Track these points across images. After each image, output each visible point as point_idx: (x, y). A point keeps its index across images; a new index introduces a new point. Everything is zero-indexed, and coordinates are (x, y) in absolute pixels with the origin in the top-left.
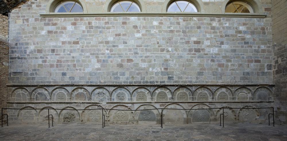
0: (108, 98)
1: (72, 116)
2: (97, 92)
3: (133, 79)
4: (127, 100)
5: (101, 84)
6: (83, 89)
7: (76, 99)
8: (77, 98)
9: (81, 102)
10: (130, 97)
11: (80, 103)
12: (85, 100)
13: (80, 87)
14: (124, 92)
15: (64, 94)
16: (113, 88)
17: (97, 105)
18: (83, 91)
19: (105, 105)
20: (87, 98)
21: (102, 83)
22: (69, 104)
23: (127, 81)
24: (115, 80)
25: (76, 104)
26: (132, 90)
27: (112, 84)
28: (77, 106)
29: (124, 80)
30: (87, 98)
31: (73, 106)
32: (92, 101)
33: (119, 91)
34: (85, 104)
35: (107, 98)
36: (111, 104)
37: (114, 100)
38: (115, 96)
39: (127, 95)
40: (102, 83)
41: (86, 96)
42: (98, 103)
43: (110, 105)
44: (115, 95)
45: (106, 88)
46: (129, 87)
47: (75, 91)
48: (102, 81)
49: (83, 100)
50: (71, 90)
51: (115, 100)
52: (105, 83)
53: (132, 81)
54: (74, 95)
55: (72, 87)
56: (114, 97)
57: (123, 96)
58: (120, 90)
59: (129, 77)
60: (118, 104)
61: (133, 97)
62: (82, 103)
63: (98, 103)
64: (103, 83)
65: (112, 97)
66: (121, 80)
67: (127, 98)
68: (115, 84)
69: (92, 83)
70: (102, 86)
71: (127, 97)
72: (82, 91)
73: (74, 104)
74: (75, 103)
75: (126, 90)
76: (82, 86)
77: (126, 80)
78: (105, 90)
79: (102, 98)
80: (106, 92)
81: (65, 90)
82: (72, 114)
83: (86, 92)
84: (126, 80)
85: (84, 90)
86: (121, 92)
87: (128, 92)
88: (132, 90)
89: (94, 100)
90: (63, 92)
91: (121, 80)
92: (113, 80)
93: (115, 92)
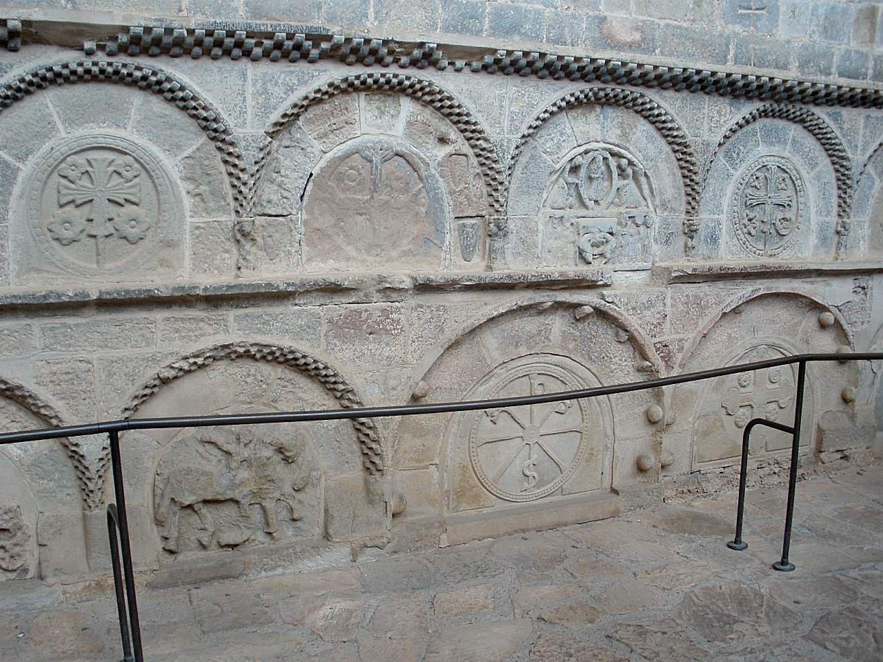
0: (666, 224)
1: (279, 470)
2: (568, 152)
3: (872, 40)
4: (813, 240)
5: (601, 56)
6: (407, 106)
7: (316, 235)
8: (325, 222)
9: (402, 273)
10: (833, 219)
11: (389, 291)
12: (428, 242)
13: (392, 71)
14: (797, 160)
15: (146, 168)
16: (726, 114)
17: (576, 306)
18: (409, 124)
19: (650, 305)
20: (450, 224)
21: (620, 46)
22: (231, 315)
23: (828, 55)
24: (738, 28)
25: (338, 307)
26: (864, 150)
27: (706, 67)
28: (348, 328)
29: (806, 40)
30: (450, 224)
31: (286, 343)
32: (512, 265)
33: (762, 149)
34: (456, 299)
35: (656, 220)
36: (704, 289)
37: (714, 240)
38: (725, 202)
39: (812, 192)
40: (620, 46)
41: (437, 200)
42: (591, 285)
43: (697, 301)
44: (730, 189)
45: (667, 103)
46: (847, 113)
47: (305, 130)
48: (622, 23)
49: (406, 245)
50: (266, 109)
51: (724, 239)
52: (645, 51)
53: (863, 56)
54: (295, 182)
55: (281, 72)
56: (718, 209)
57: (783, 197)
58: (771, 138)
59: (845, 11)
60: (763, 287)
61: (852, 221)
62: (425, 287)
63: (591, 285)
64: (631, 46)
65: (704, 217)
66: (782, 33)
67: (814, 226)
68: (737, 71)
69: (513, 29)
70: (629, 78)
71: (813, 217)
72: (400, 126)
73: (312, 307)
74: (333, 289)
75: (810, 142)
76: (427, 58)
77: (816, 37)
78: (643, 128)
79: (611, 223)
80: (652, 150)
81: (156, 105)
82: (280, 450)
83: (443, 140)
84: (820, 42)
85: (427, 114)
86: (772, 163)
87: (824, 162)
88: (864, 150)
89: (527, 247)
90: (129, 135)
91: (782, 33)
92: (719, 26)
93: (730, 158)
